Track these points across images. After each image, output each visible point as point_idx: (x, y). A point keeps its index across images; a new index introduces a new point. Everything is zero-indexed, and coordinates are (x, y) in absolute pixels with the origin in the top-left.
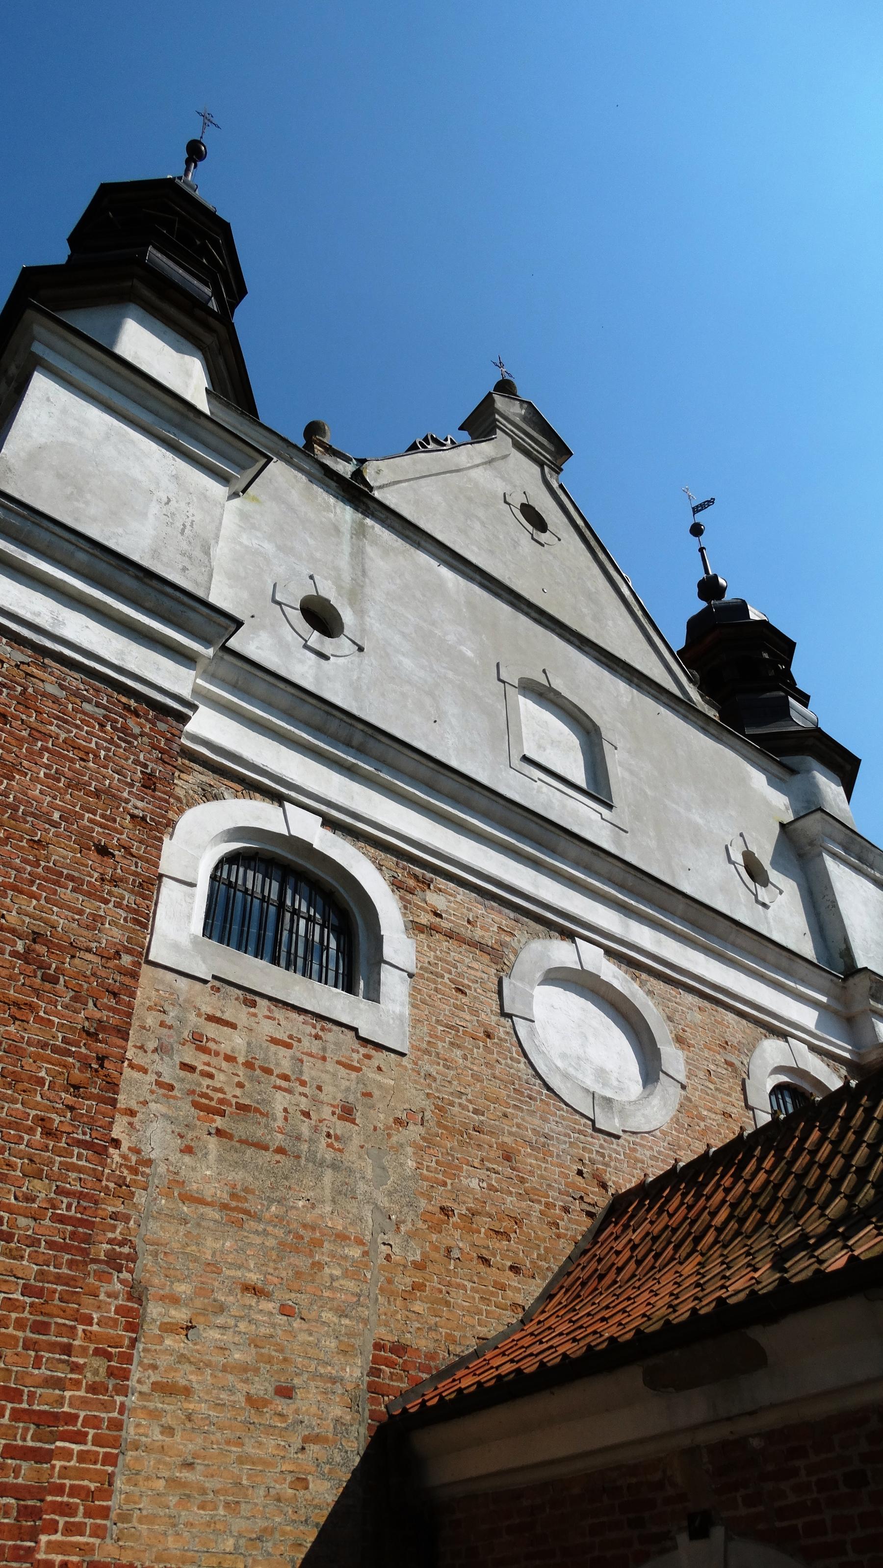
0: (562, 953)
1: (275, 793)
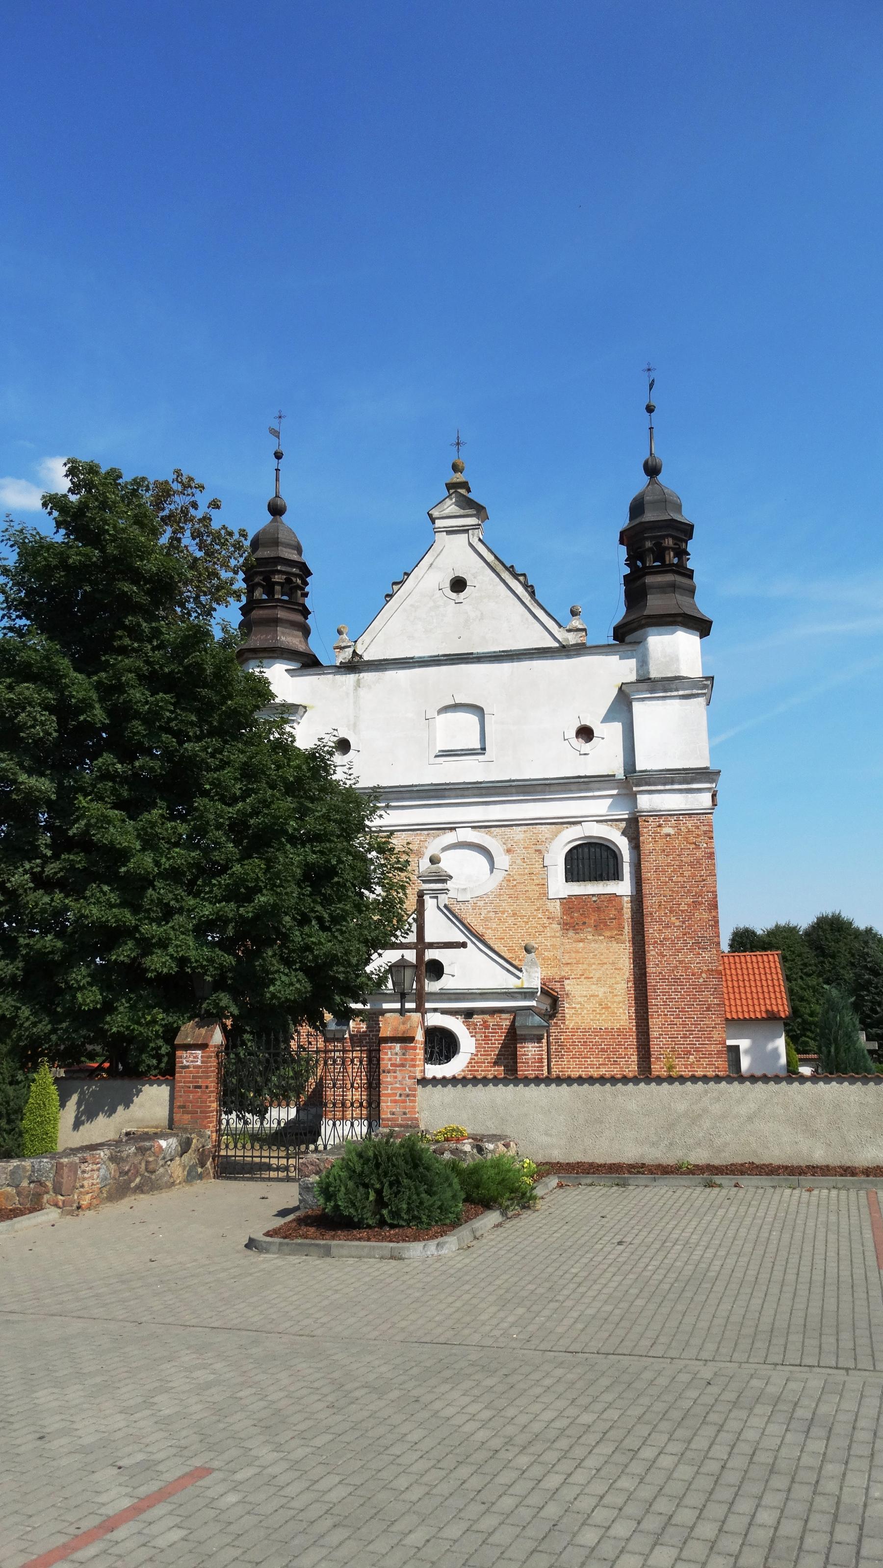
0: (450, 838)
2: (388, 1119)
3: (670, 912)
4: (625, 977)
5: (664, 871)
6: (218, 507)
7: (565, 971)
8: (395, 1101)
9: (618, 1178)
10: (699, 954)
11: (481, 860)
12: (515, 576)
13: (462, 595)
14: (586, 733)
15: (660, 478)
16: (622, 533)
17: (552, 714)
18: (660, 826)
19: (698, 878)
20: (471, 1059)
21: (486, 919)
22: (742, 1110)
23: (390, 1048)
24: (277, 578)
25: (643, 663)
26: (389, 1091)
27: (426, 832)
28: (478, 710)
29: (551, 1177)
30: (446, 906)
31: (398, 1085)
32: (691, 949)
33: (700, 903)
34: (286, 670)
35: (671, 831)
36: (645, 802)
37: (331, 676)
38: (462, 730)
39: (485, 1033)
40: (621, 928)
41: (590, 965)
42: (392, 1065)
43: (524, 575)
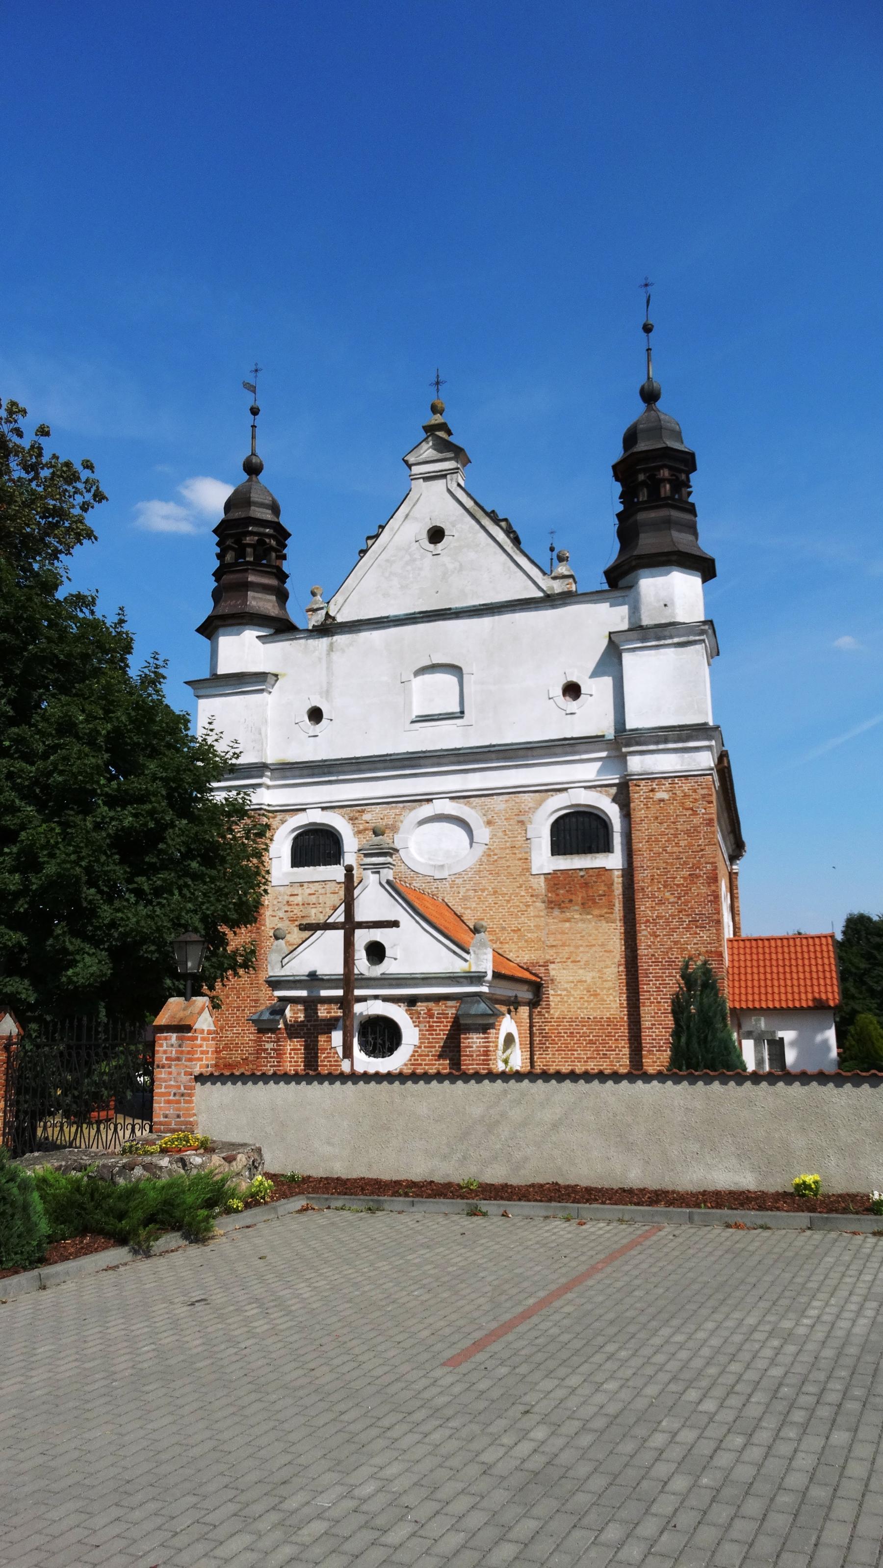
0: (426, 810)
1: (300, 809)
2: (161, 1123)
3: (665, 886)
4: (616, 960)
5: (657, 840)
6: (47, 434)
7: (550, 954)
8: (168, 1102)
9: (372, 1200)
10: (696, 933)
11: (460, 833)
12: (496, 520)
13: (440, 546)
14: (572, 690)
15: (659, 404)
16: (615, 467)
17: (537, 671)
18: (652, 790)
19: (696, 848)
20: (415, 1051)
21: (465, 898)
22: (547, 1115)
23: (166, 1039)
24: (248, 540)
25: (635, 610)
26: (163, 1090)
27: (401, 805)
28: (455, 670)
29: (301, 1196)
30: (388, 882)
31: (172, 1083)
32: (688, 929)
33: (698, 876)
34: (257, 637)
35: (665, 796)
36: (636, 764)
37: (302, 641)
38: (439, 693)
39: (429, 1022)
40: (611, 906)
41: (577, 947)
42: (167, 1059)
43: (506, 520)
